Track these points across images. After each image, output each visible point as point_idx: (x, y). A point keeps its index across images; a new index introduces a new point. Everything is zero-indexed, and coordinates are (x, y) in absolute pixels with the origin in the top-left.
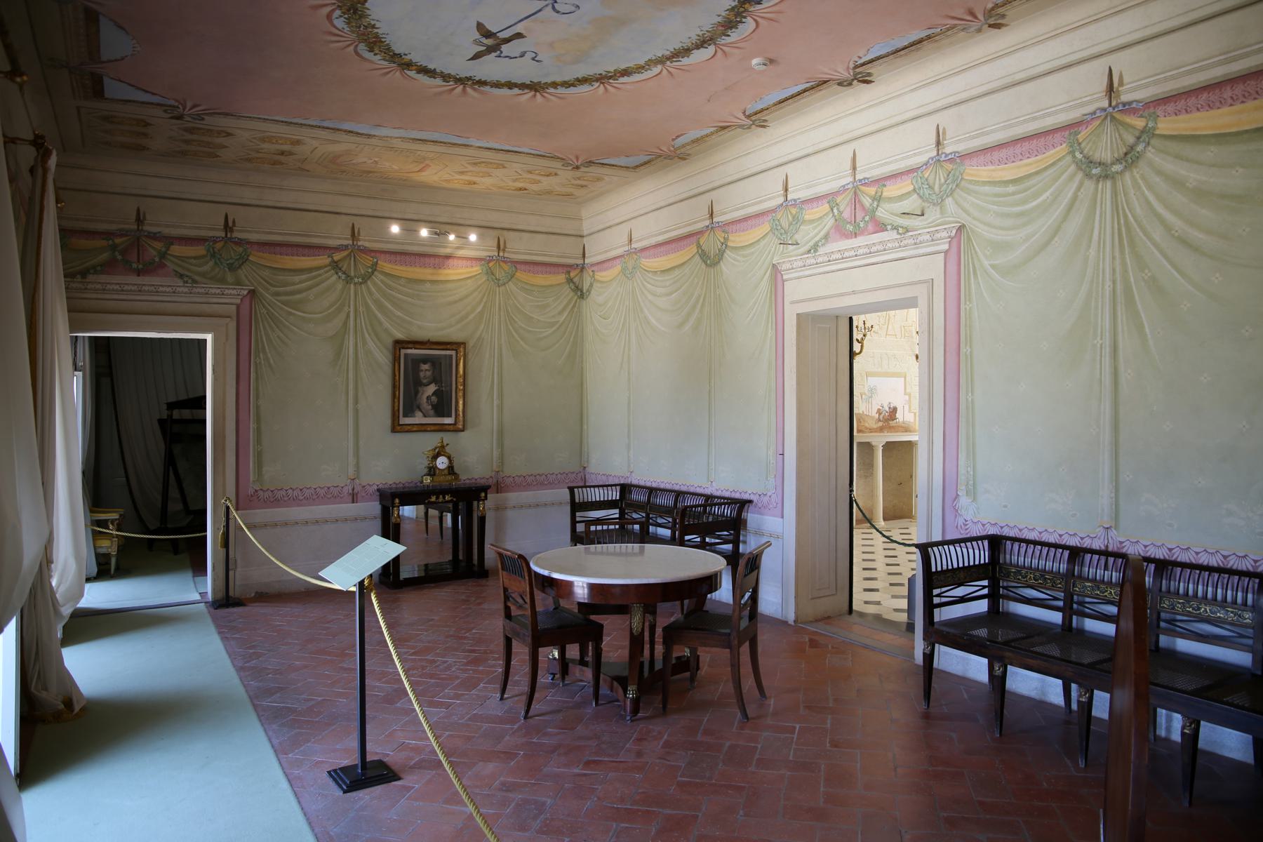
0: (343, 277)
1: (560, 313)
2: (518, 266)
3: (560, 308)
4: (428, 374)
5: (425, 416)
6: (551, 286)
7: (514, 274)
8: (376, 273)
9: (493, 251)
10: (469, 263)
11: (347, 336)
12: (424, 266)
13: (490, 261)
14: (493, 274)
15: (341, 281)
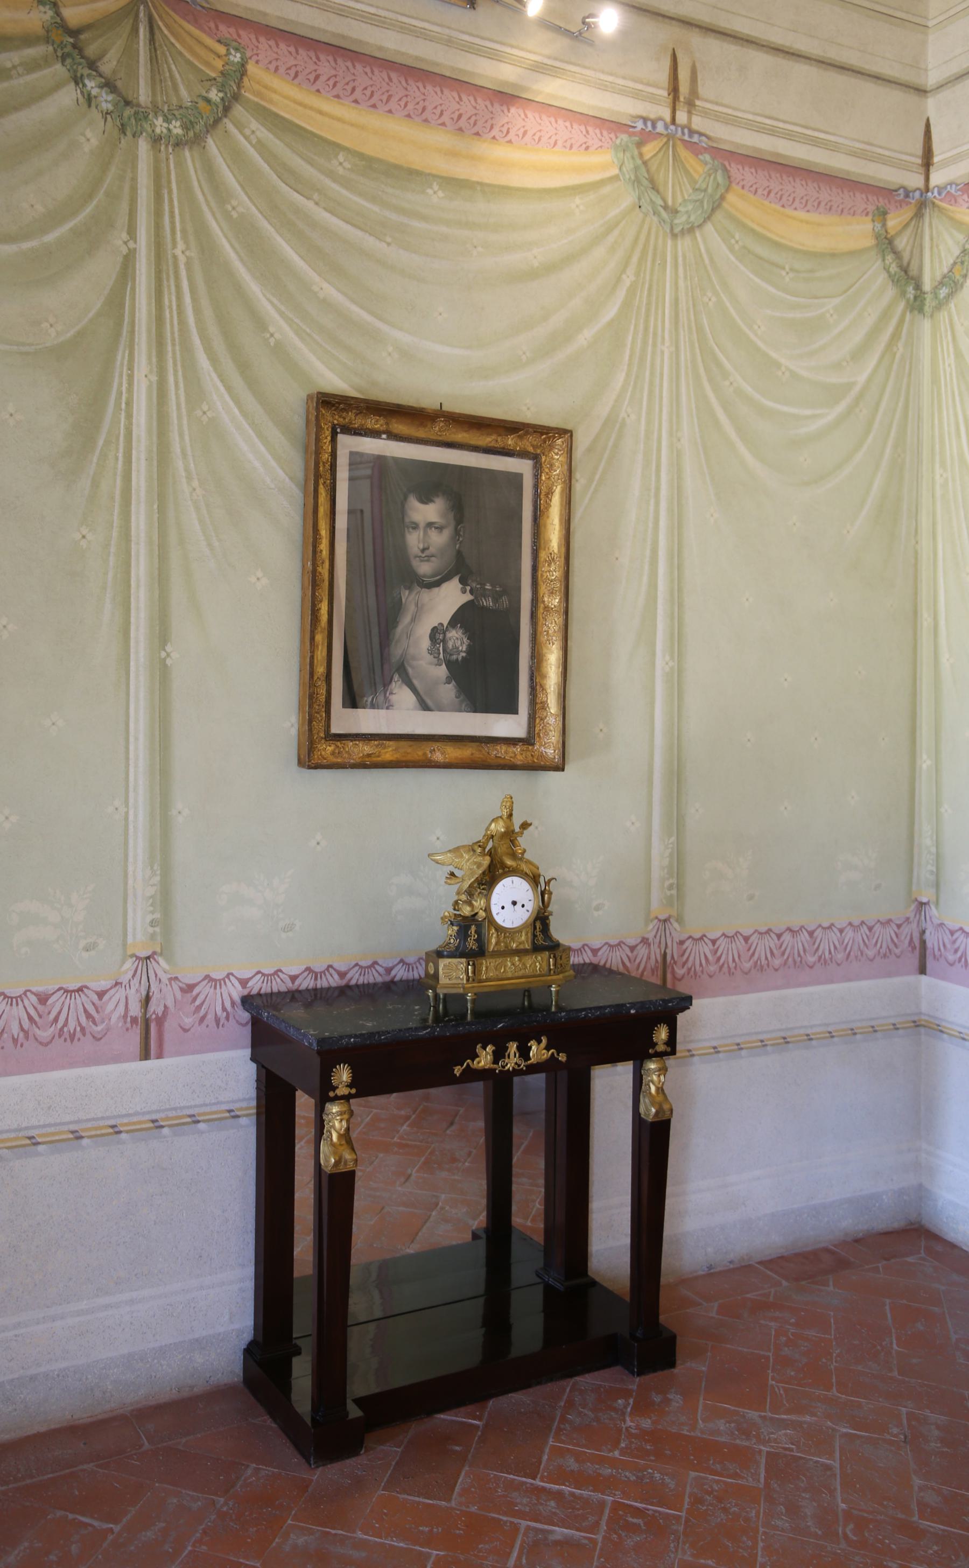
0: (106, 100)
1: (858, 355)
2: (734, 169)
3: (858, 337)
4: (439, 540)
5: (425, 707)
6: (833, 255)
7: (722, 198)
8: (238, 110)
9: (652, 99)
10: (577, 134)
11: (121, 356)
12: (420, 116)
13: (644, 138)
14: (655, 188)
15: (95, 115)
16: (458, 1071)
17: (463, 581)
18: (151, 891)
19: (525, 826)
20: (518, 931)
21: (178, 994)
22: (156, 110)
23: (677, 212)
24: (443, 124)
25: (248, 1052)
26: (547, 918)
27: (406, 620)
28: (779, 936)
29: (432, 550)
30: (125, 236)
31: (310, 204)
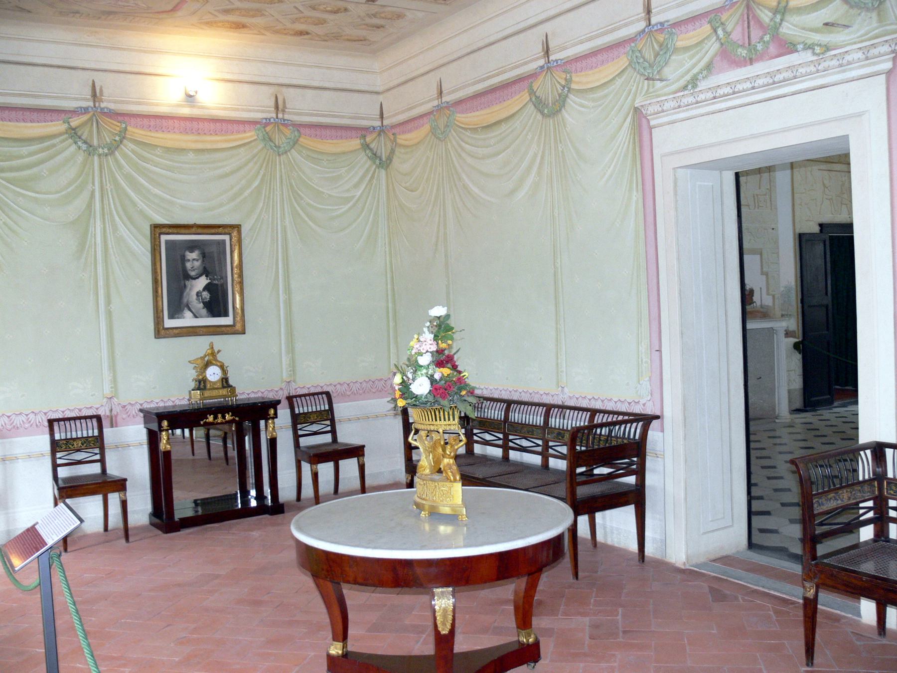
0: (84, 147)
1: (356, 186)
2: (302, 130)
3: (356, 180)
4: (197, 264)
5: (196, 317)
6: (344, 153)
7: (298, 140)
8: (125, 141)
9: (269, 112)
11: (92, 221)
13: (267, 125)
14: (271, 140)
15: (81, 152)
16: (202, 423)
17: (207, 276)
18: (110, 378)
19: (219, 351)
20: (218, 381)
21: (121, 409)
22: (99, 146)
23: (280, 147)
24: (193, 133)
25: (143, 426)
26: (227, 378)
27: (188, 290)
28: (335, 386)
29: (195, 267)
30: (91, 185)
31: (149, 165)
